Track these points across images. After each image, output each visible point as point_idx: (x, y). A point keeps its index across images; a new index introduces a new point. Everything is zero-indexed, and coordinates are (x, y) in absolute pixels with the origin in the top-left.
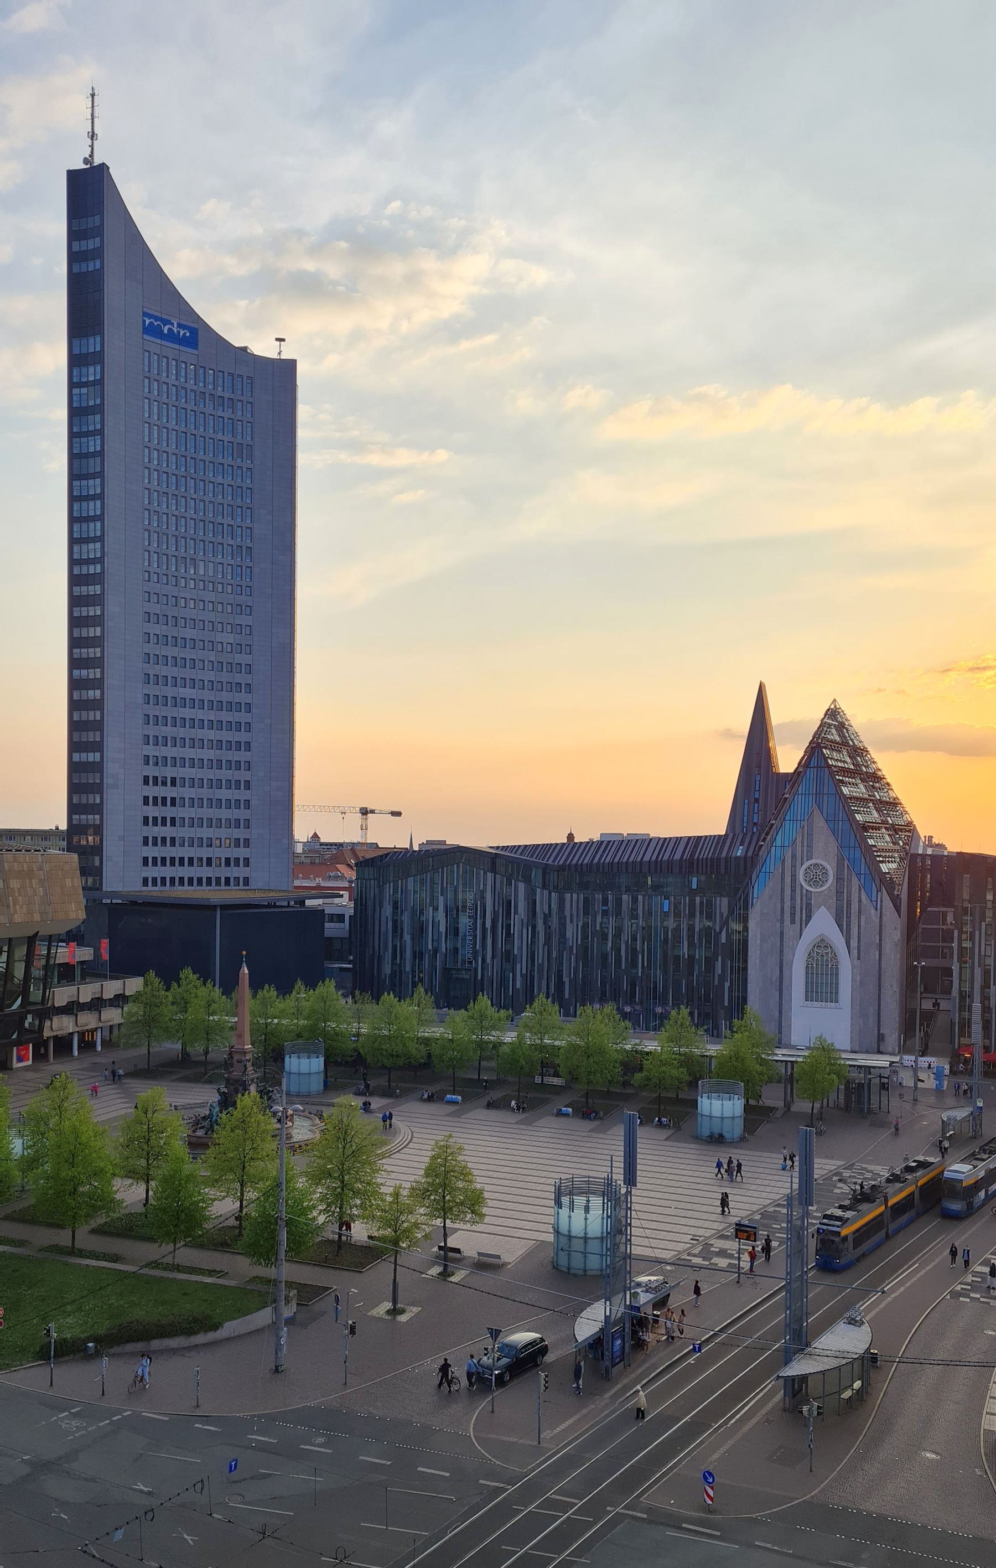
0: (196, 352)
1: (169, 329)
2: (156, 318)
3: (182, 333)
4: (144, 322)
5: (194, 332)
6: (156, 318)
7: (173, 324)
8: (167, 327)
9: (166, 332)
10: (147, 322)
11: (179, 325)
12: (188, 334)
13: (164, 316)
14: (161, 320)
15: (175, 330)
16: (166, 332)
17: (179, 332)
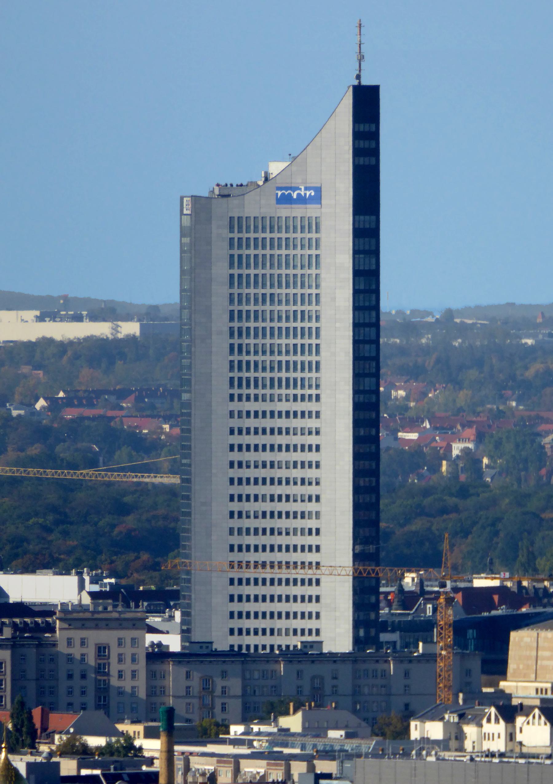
0: (319, 206)
1: (299, 195)
2: (286, 189)
3: (308, 193)
4: (277, 194)
5: (318, 190)
6: (286, 189)
7: (300, 189)
8: (296, 193)
9: (295, 197)
10: (280, 193)
11: (306, 189)
12: (313, 194)
13: (293, 185)
14: (291, 188)
15: (303, 193)
16: (295, 197)
17: (305, 194)
